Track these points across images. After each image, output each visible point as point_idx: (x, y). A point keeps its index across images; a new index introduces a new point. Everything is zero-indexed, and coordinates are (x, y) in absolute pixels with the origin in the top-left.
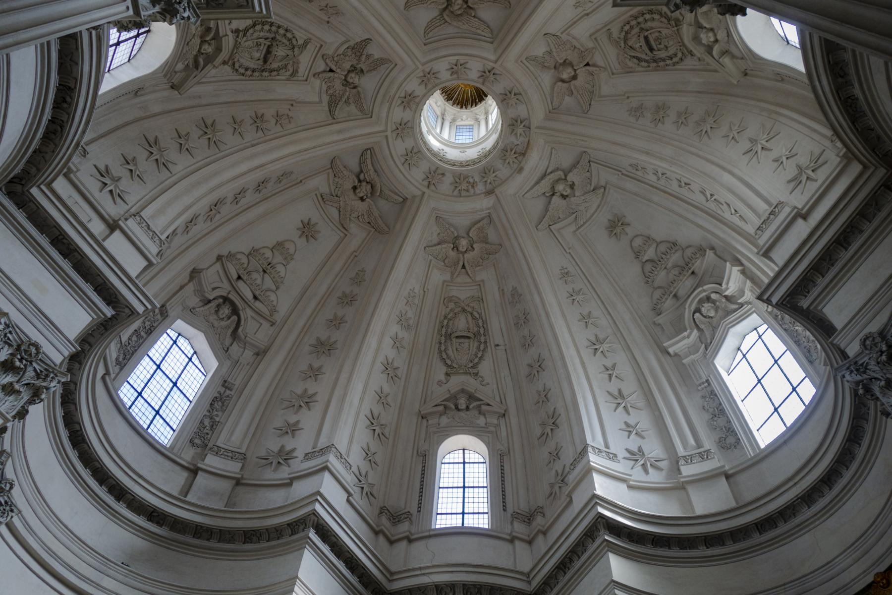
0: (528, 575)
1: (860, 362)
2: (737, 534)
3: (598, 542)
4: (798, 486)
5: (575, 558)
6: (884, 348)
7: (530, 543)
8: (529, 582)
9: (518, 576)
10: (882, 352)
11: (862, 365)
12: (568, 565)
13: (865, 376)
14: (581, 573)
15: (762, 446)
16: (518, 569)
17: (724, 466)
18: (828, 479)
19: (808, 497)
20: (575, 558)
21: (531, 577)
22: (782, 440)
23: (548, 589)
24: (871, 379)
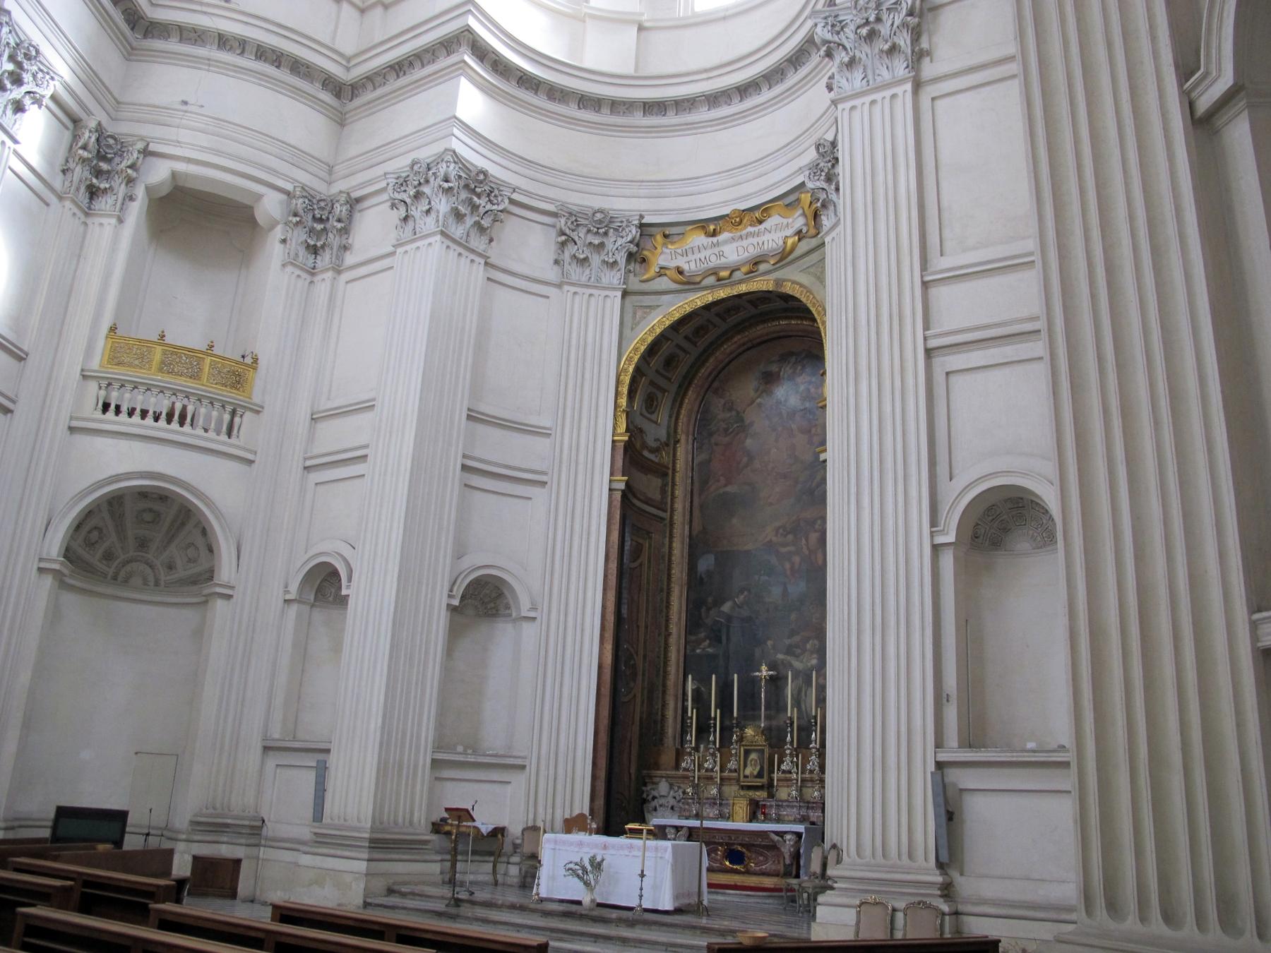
0: (349, 60)
1: (841, 18)
2: (616, 106)
3: (454, 58)
4: (710, 81)
5: (417, 64)
6: (872, 19)
7: (363, 11)
8: (348, 69)
9: (335, 57)
10: (867, 22)
11: (840, 22)
12: (405, 68)
13: (836, 38)
14: (419, 85)
15: (698, 9)
16: (336, 47)
17: (642, 14)
18: (744, 90)
19: (714, 99)
20: (417, 64)
21: (353, 63)
22: (722, 14)
23: (370, 86)
24: (839, 45)
